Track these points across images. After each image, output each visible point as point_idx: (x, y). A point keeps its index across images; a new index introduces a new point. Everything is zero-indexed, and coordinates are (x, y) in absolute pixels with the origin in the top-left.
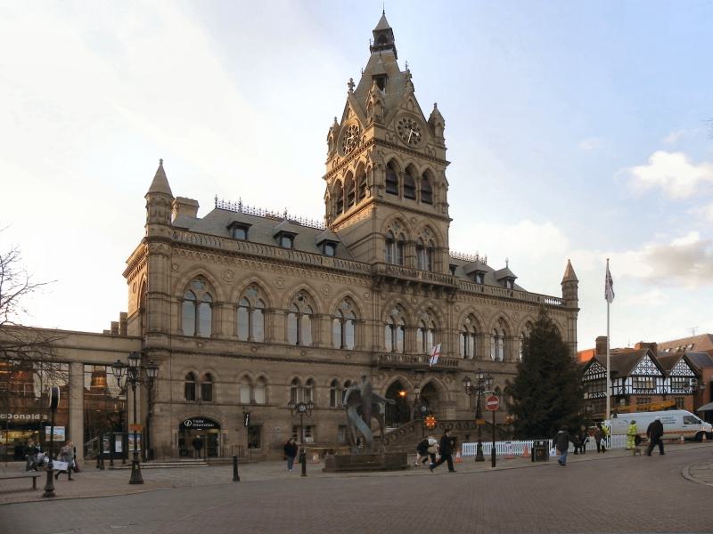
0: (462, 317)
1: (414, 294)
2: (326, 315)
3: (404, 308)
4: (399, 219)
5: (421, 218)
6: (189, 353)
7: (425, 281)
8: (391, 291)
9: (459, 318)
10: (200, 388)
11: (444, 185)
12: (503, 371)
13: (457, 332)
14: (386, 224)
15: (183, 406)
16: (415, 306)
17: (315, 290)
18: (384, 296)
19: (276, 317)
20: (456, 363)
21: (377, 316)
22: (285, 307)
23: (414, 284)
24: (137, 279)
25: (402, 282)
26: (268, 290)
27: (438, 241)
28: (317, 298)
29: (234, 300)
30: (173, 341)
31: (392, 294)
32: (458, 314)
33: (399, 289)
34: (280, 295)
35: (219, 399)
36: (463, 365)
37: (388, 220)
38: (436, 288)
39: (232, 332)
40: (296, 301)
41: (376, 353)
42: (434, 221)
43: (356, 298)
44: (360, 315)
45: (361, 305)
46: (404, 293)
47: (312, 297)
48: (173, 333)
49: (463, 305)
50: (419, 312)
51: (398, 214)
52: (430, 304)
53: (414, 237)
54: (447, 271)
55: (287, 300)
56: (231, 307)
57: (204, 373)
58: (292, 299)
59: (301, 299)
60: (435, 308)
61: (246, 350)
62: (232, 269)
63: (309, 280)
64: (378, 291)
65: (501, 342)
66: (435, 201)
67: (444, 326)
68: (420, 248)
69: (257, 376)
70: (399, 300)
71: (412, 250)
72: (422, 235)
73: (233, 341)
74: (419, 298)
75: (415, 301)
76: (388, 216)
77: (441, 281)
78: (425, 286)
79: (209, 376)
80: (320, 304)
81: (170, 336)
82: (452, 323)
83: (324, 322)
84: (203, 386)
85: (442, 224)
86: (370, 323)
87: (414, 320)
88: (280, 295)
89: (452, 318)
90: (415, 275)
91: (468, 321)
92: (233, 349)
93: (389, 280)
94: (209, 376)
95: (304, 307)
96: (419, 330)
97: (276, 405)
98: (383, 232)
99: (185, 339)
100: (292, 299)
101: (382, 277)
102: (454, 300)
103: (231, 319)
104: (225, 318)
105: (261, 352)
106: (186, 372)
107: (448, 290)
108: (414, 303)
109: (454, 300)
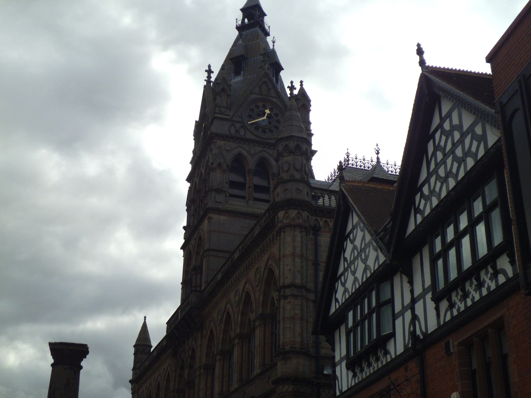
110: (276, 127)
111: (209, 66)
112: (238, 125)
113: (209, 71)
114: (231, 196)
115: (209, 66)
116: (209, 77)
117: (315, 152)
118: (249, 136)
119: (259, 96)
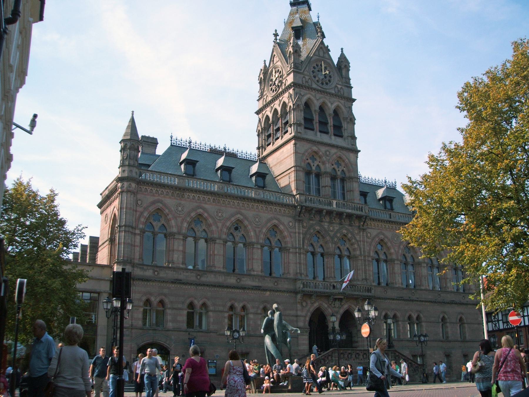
0: (374, 243)
1: (331, 223)
2: (257, 244)
3: (322, 236)
4: (316, 153)
5: (333, 151)
6: (147, 280)
7: (341, 210)
8: (311, 219)
9: (370, 245)
10: (155, 314)
11: (352, 120)
12: (414, 298)
13: (370, 259)
14: (304, 158)
15: (141, 331)
16: (332, 234)
17: (248, 221)
18: (305, 224)
19: (216, 245)
20: (369, 290)
21: (299, 244)
22: (224, 236)
23: (330, 213)
24: (109, 211)
25: (320, 211)
26: (210, 221)
27: (349, 171)
28: (250, 227)
29: (184, 231)
30: (135, 269)
31: (311, 222)
32: (370, 240)
33: (318, 218)
34: (220, 225)
35: (170, 325)
36: (377, 292)
37: (306, 154)
38: (350, 216)
39: (181, 260)
40: (232, 230)
41: (300, 280)
42: (344, 152)
43: (281, 227)
44: (286, 243)
45: (286, 233)
46: (322, 222)
47: (246, 227)
48: (136, 261)
49: (374, 232)
50: (336, 239)
51: (315, 148)
52: (345, 231)
53: (328, 168)
54: (357, 198)
55: (225, 230)
56: (181, 237)
57: (158, 300)
58: (229, 229)
59: (236, 229)
60: (350, 235)
61: (192, 277)
62: (183, 202)
63: (243, 211)
64: (300, 220)
65: (410, 268)
66: (345, 134)
67: (358, 253)
68: (333, 178)
69: (201, 303)
70: (318, 228)
71: (326, 181)
72: (335, 166)
73: (182, 269)
74: (335, 225)
75: (331, 228)
76: (306, 151)
77: (354, 208)
78: (340, 215)
79: (162, 302)
80: (252, 234)
81: (133, 265)
82: (364, 248)
83: (255, 250)
84: (158, 312)
85: (352, 155)
86: (294, 250)
87: (331, 247)
88: (220, 225)
89: (364, 245)
90: (330, 204)
91: (379, 247)
92: (182, 276)
93: (309, 210)
94: (162, 302)
95: (238, 235)
96: (336, 256)
97: (215, 332)
98: (303, 165)
99: (145, 267)
100: (229, 229)
101: (302, 207)
102: (365, 227)
103: (181, 248)
104: (175, 248)
105: (205, 279)
106: (144, 298)
107: (359, 217)
108: (332, 231)
109: (365, 227)
110: (330, 81)
111: (276, 31)
112: (307, 77)
113: (276, 35)
114: (305, 128)
115: (276, 31)
116: (276, 39)
117: (354, 100)
118: (314, 86)
119: (317, 57)
